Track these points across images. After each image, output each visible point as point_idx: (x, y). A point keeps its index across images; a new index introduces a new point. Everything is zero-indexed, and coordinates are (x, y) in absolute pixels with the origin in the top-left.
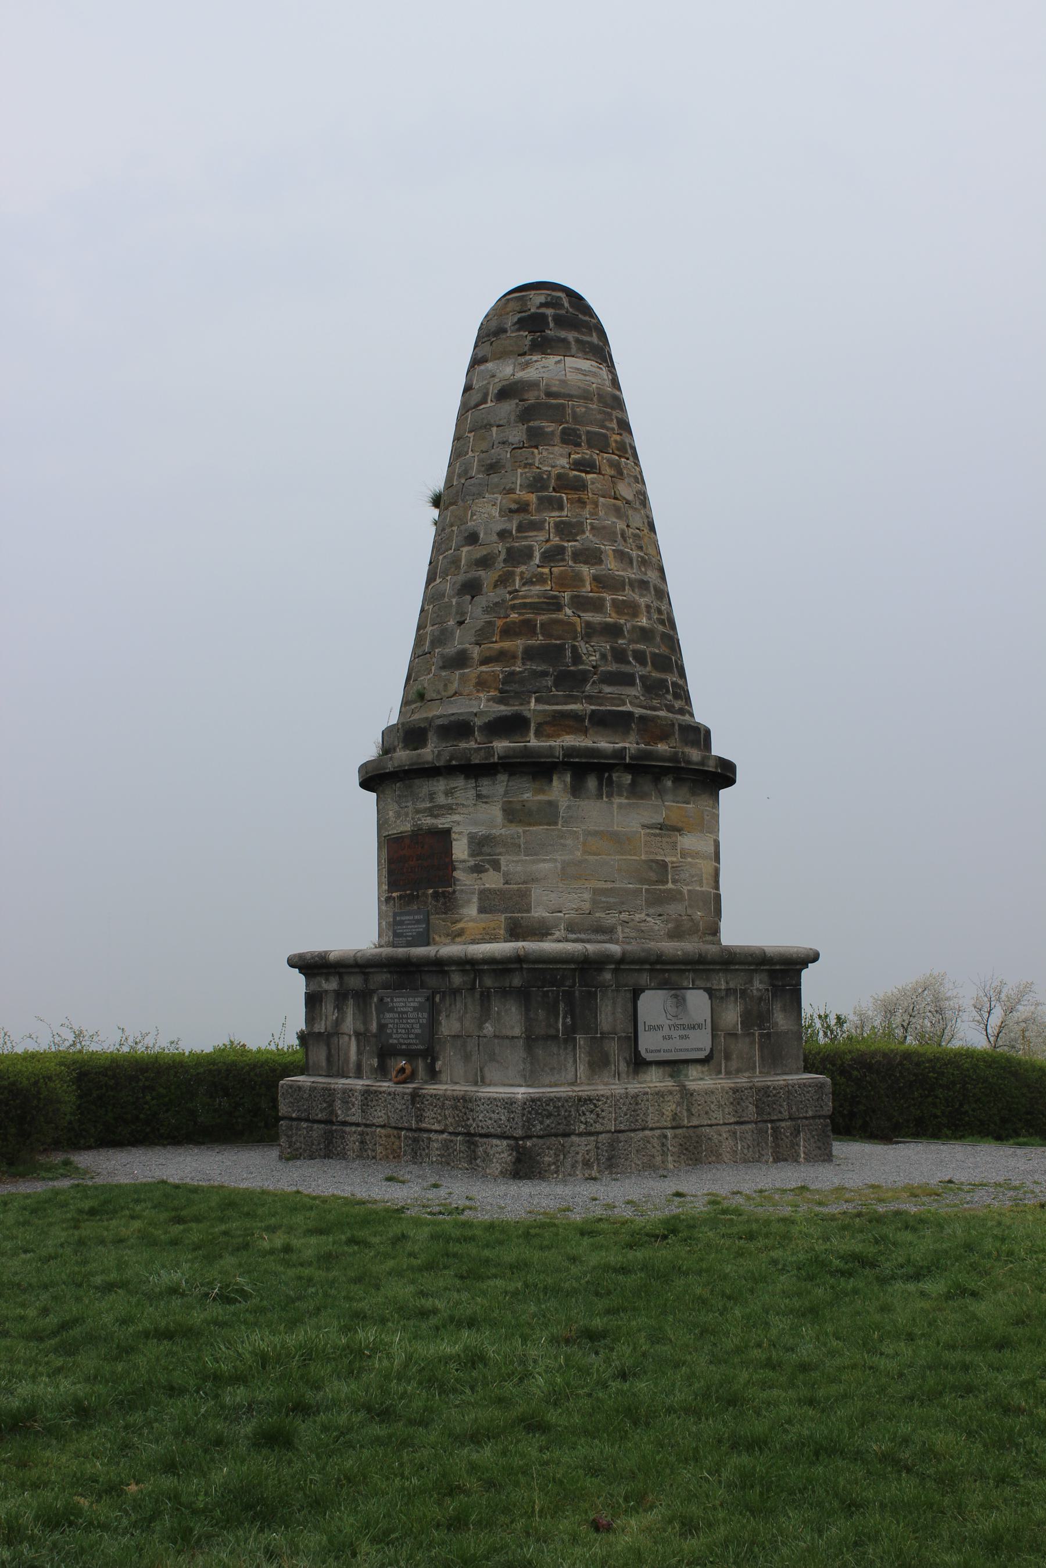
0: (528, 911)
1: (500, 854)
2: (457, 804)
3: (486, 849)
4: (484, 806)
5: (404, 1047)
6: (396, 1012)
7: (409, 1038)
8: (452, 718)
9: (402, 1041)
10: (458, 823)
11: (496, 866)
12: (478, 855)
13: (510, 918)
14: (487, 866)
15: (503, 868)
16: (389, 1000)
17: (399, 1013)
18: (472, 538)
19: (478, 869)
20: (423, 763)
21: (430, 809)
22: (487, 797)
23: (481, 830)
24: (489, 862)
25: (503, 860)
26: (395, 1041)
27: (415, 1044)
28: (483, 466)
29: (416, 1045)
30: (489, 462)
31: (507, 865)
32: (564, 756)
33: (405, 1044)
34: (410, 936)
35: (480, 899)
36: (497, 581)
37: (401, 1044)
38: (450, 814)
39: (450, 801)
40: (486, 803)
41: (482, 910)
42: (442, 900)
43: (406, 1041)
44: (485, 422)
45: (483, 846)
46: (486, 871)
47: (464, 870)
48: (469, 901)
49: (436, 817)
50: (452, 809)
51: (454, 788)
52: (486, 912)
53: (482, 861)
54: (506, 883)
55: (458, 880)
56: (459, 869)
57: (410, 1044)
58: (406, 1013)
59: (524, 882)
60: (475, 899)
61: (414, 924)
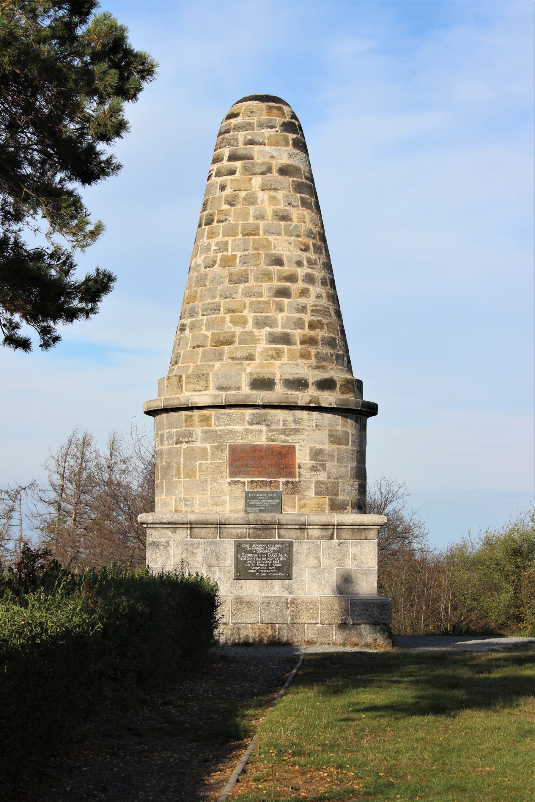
0: (338, 495)
1: (326, 461)
2: (302, 429)
3: (319, 457)
4: (319, 431)
5: (263, 574)
6: (254, 553)
7: (268, 569)
8: (296, 376)
9: (262, 571)
10: (303, 440)
11: (324, 467)
12: (314, 460)
13: (331, 499)
14: (320, 468)
15: (327, 469)
16: (247, 546)
17: (258, 554)
18: (278, 262)
19: (314, 469)
20: (288, 403)
21: (282, 430)
22: (321, 427)
23: (318, 446)
24: (321, 465)
25: (328, 464)
26: (253, 571)
27: (273, 573)
28: (277, 216)
29: (277, 573)
30: (281, 214)
31: (329, 468)
32: (362, 407)
33: (265, 573)
34: (264, 507)
35: (316, 487)
36: (301, 293)
37: (260, 573)
38: (298, 434)
39: (297, 426)
40: (319, 429)
41: (317, 494)
42: (291, 486)
43: (265, 571)
44: (273, 187)
45: (317, 455)
46: (320, 470)
47: (306, 469)
48: (309, 488)
49: (287, 435)
50: (299, 432)
51: (300, 419)
52: (318, 495)
53: (317, 464)
54: (329, 478)
55: (303, 475)
56: (303, 468)
57: (269, 573)
58: (266, 554)
59: (337, 478)
60: (313, 486)
61: (268, 500)
